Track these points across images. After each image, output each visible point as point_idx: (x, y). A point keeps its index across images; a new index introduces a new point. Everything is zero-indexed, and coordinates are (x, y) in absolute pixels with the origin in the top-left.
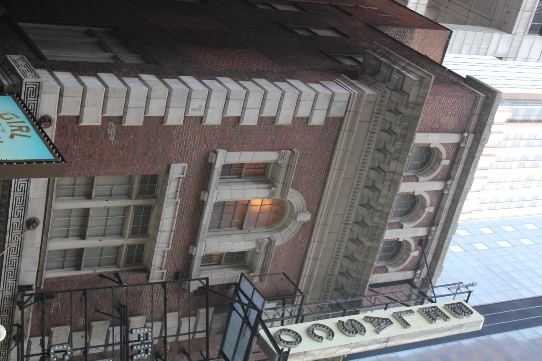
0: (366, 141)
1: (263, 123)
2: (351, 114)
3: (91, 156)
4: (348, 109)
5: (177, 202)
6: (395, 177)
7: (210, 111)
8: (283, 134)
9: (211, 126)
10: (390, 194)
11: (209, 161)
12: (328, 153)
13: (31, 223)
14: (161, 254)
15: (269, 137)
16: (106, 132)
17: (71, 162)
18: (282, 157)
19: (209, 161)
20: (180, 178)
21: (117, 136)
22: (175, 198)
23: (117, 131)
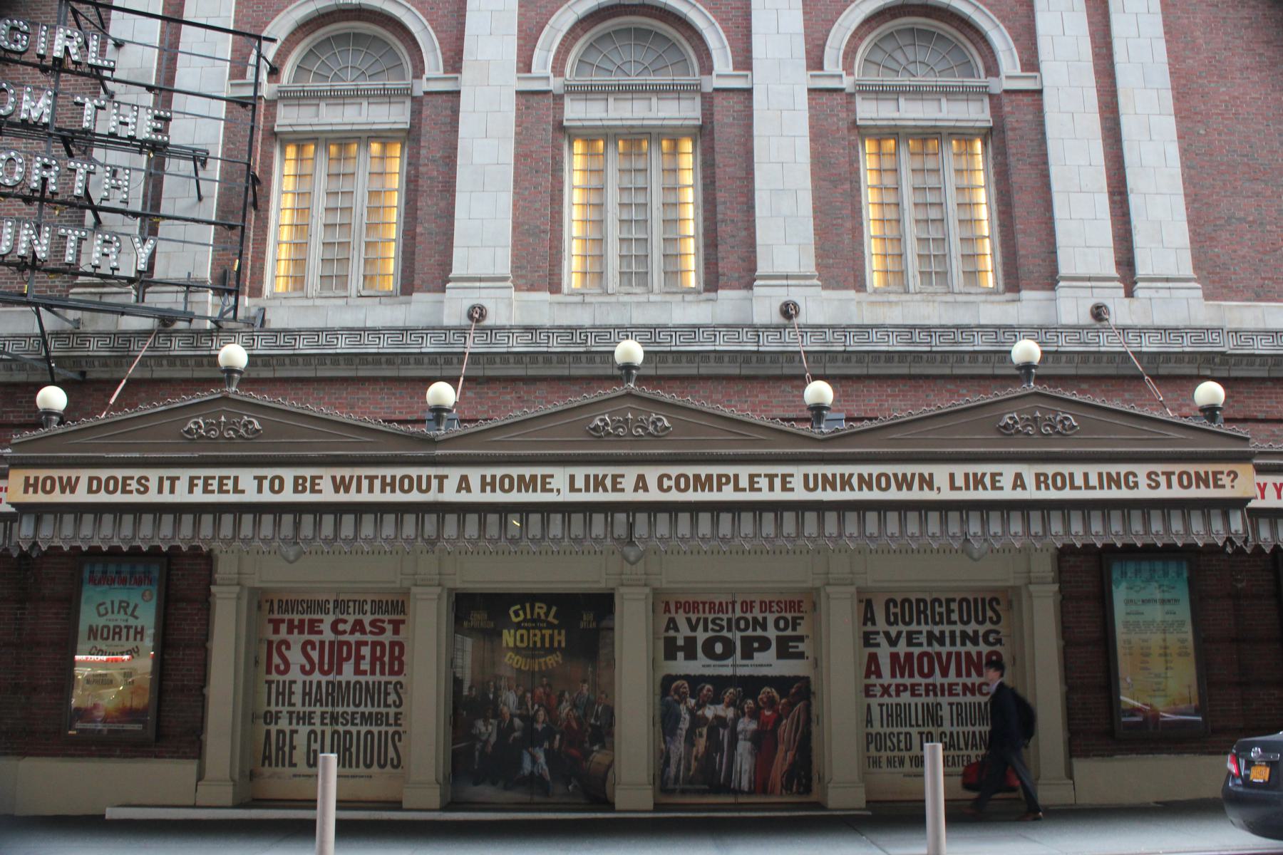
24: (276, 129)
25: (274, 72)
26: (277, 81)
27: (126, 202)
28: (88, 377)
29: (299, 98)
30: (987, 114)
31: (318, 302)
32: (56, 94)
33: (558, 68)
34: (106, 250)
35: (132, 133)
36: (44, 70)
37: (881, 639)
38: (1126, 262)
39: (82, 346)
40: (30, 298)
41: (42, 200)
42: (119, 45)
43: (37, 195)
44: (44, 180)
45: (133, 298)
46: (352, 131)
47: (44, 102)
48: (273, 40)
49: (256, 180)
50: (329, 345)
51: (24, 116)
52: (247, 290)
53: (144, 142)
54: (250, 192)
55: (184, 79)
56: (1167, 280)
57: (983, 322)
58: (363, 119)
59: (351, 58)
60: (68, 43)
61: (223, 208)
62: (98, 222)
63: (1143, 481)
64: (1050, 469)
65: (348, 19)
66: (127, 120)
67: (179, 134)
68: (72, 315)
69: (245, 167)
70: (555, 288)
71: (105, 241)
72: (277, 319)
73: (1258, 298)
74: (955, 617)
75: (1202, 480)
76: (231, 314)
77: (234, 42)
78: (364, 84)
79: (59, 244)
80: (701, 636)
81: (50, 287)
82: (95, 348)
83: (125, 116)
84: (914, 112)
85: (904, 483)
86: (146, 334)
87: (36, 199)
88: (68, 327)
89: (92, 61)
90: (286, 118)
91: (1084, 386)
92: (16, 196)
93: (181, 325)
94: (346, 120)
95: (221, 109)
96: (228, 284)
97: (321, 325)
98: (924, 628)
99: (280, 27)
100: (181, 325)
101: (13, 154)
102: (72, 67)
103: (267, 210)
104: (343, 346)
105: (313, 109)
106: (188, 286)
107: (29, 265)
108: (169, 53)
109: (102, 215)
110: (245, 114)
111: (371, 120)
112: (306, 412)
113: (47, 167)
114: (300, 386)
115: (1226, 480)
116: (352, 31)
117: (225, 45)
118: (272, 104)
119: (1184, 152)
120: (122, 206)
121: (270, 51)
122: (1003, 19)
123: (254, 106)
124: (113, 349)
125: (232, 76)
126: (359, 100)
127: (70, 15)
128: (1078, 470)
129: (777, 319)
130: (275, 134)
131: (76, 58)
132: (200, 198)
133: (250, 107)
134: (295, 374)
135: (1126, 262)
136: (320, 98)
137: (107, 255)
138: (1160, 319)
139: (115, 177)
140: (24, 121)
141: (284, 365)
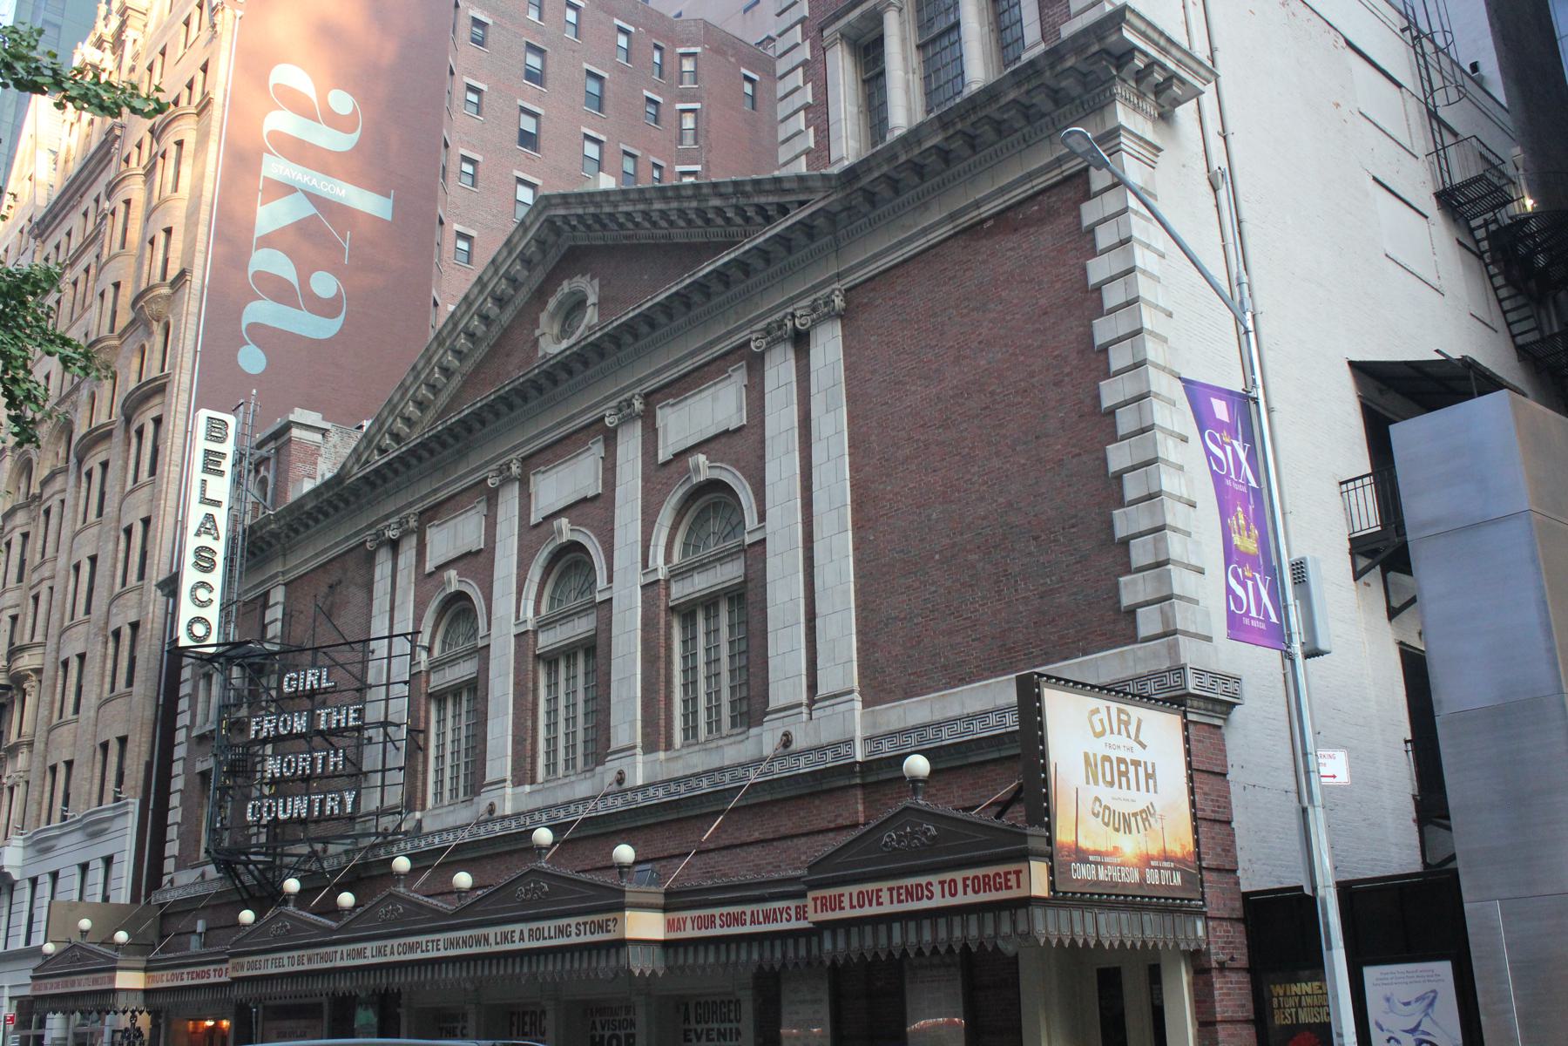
13: (203, 875)
25: (429, 650)
30: (742, 572)
33: (537, 611)
37: (693, 1036)
38: (812, 687)
56: (836, 696)
57: (727, 763)
63: (574, 930)
64: (534, 925)
70: (533, 781)
73: (907, 696)
74: (732, 1016)
75: (601, 927)
80: (607, 1034)
84: (700, 583)
85: (478, 943)
90: (438, 681)
91: (775, 810)
98: (715, 1026)
107: (302, 822)
115: (611, 927)
119: (858, 562)
122: (748, 477)
128: (545, 924)
129: (615, 787)
135: (812, 687)
138: (825, 737)
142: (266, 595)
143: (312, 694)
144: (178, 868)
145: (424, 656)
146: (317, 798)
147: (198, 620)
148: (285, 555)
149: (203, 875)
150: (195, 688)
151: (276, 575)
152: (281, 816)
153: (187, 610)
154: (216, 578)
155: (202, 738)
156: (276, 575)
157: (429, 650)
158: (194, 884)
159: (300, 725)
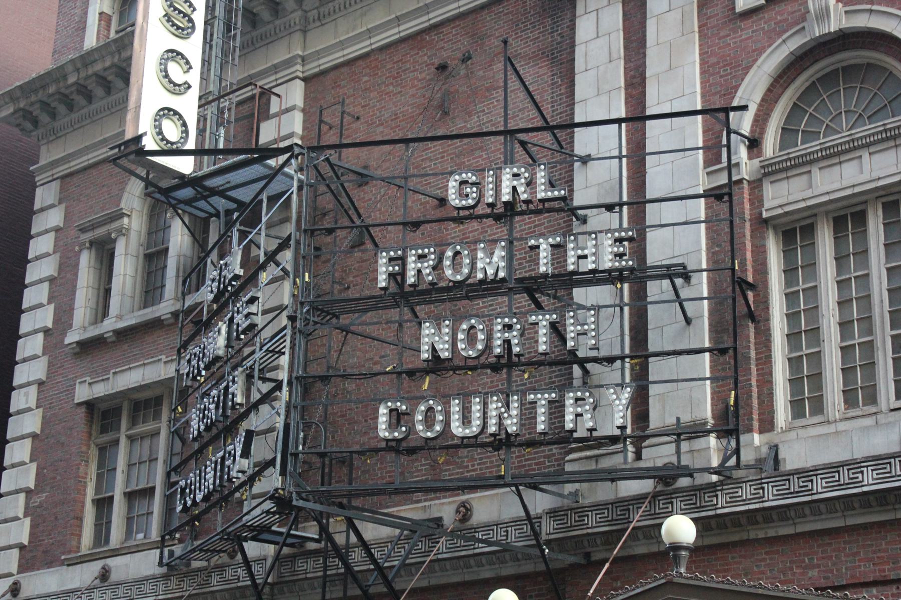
0: (84, 123)
1: (56, 294)
2: (55, 171)
3: (56, 518)
4: (50, 179)
5: (114, 373)
6: (79, 65)
7: (31, 379)
8: (68, 258)
9: (49, 367)
10: (97, 57)
11: (78, 350)
12: (94, 172)
13: (104, 575)
14: (169, 365)
15: (68, 275)
16: (38, 507)
17: (59, 541)
18: (82, 246)
19: (78, 350)
20: (90, 384)
21: (43, 491)
22: (108, 379)
23: (37, 494)
24: (765, 215)
25: (754, 144)
26: (760, 154)
27: (595, 348)
28: (593, 559)
29: (786, 169)
31: (842, 426)
32: (511, 242)
34: (579, 409)
35: (592, 266)
36: (497, 218)
39: (581, 524)
40: (508, 479)
41: (510, 365)
42: (585, 160)
43: (503, 361)
44: (507, 342)
45: (631, 456)
46: (854, 195)
47: (499, 252)
48: (744, 108)
49: (741, 285)
50: (854, 483)
51: (480, 276)
52: (756, 424)
53: (609, 271)
54: (740, 301)
55: (658, 180)
58: (865, 177)
59: (846, 100)
60: (515, 183)
61: (716, 329)
62: (586, 372)
65: (832, 54)
66: (586, 252)
67: (660, 249)
68: (569, 488)
69: (729, 273)
71: (577, 400)
72: (795, 456)
76: (734, 459)
77: (704, 121)
78: (859, 132)
79: (528, 413)
81: (548, 457)
82: (594, 524)
83: (583, 249)
86: (639, 499)
87: (503, 366)
88: (567, 502)
89: (541, 195)
90: (779, 197)
92: (484, 366)
93: (684, 482)
94: (845, 183)
95: (700, 208)
96: (730, 424)
97: (845, 456)
99: (752, 89)
100: (684, 482)
101: (473, 321)
102: (524, 207)
103: (768, 320)
104: (870, 481)
105: (805, 178)
106: (679, 435)
107: (503, 442)
108: (637, 156)
109: (589, 366)
110: (723, 208)
111: (875, 175)
112: (760, 591)
113: (509, 327)
114: (827, 540)
116: (839, 65)
117: (694, 131)
118: (756, 185)
120: (594, 354)
121: (745, 123)
123: (730, 195)
124: (611, 522)
125: (707, 163)
126: (857, 154)
127: (517, 145)
130: (766, 221)
131: (524, 197)
132: (688, 321)
133: (726, 198)
134: (819, 526)
136: (811, 162)
137: (581, 415)
139: (596, 321)
140: (482, 282)
141: (805, 516)
142: (266, 94)
143: (508, 212)
144: (25, 566)
145: (742, 153)
146: (542, 399)
147: (167, 112)
148: (304, 32)
149: (104, 575)
150: (68, 267)
151: (288, 63)
152: (457, 429)
153: (150, 94)
154: (193, 47)
155: (88, 347)
156: (288, 63)
157: (754, 144)
158: (90, 589)
159: (491, 263)
